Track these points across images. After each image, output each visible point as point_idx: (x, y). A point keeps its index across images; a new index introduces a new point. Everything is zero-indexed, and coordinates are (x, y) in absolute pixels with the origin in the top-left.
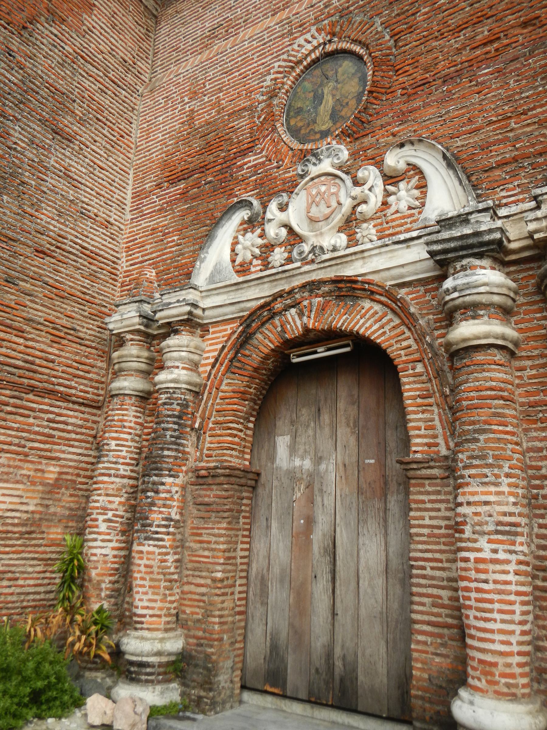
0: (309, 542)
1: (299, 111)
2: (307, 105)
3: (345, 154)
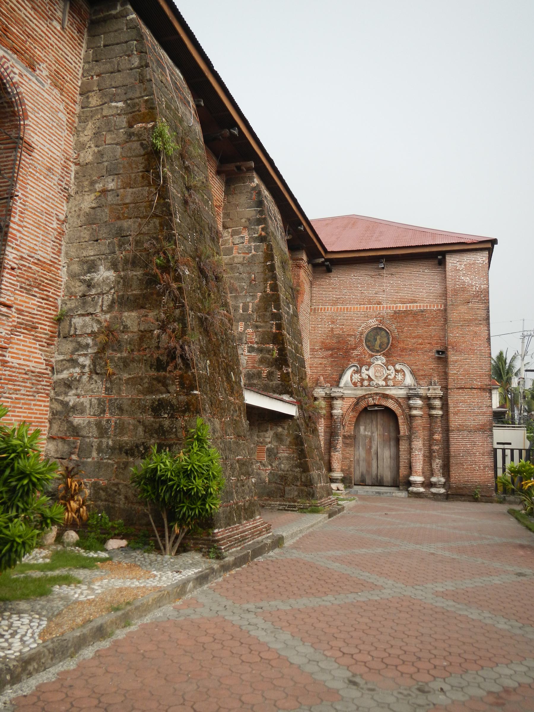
0: (371, 452)
1: (369, 341)
2: (372, 339)
3: (385, 361)
